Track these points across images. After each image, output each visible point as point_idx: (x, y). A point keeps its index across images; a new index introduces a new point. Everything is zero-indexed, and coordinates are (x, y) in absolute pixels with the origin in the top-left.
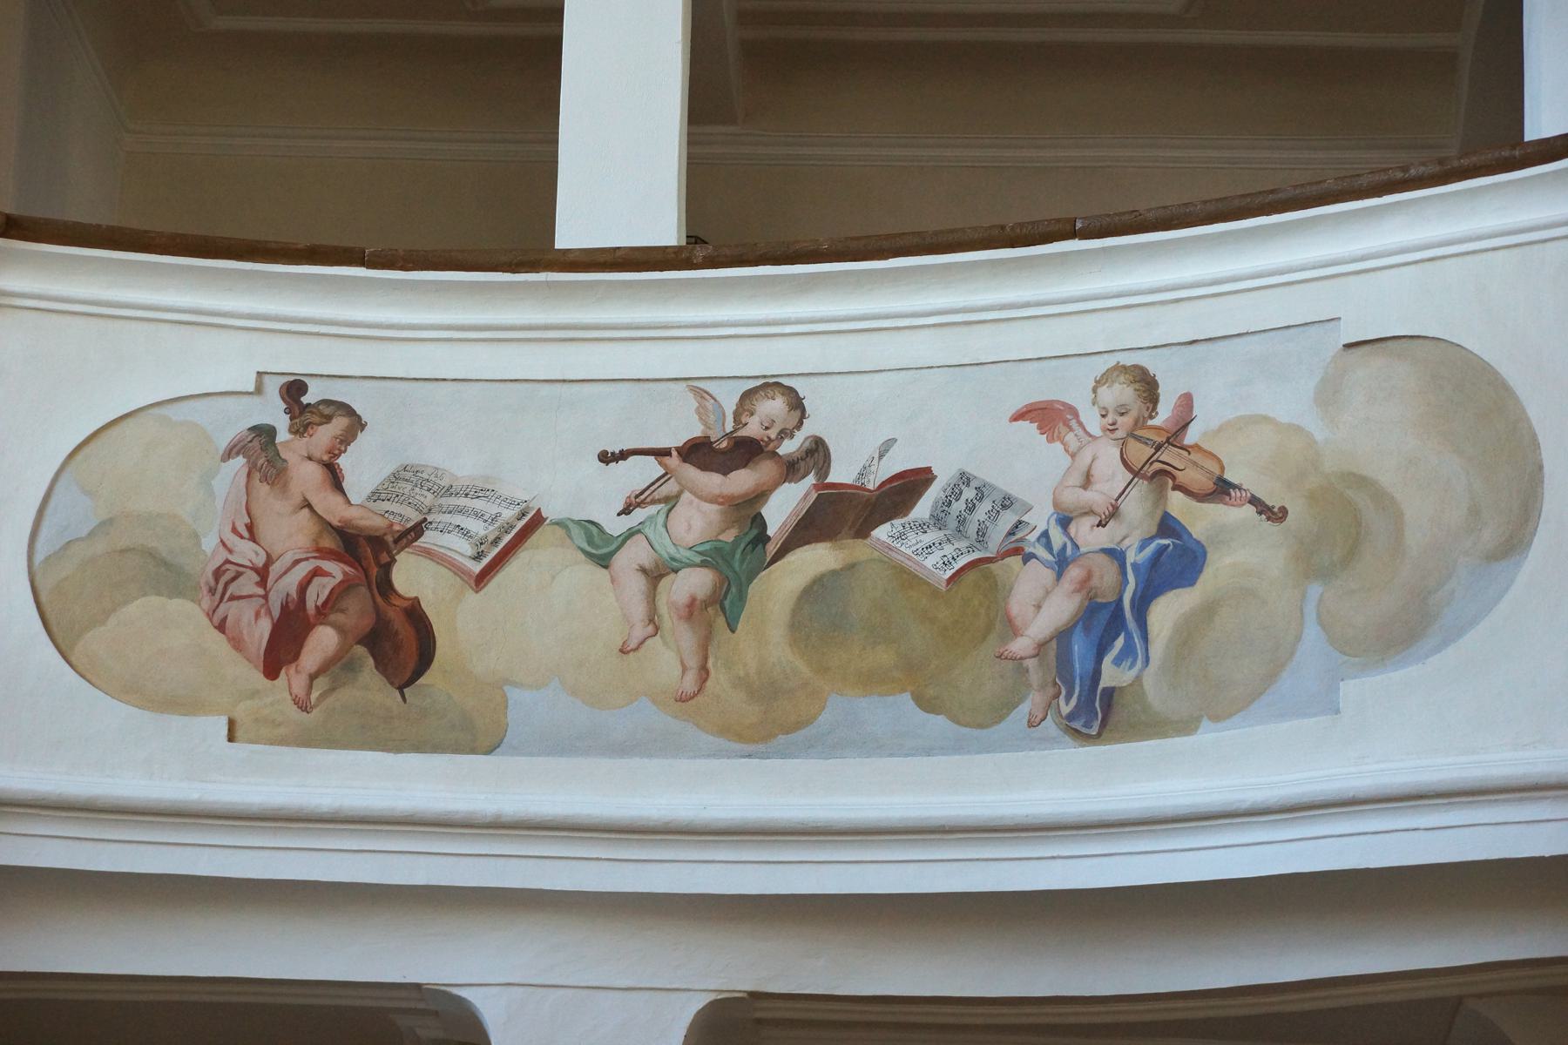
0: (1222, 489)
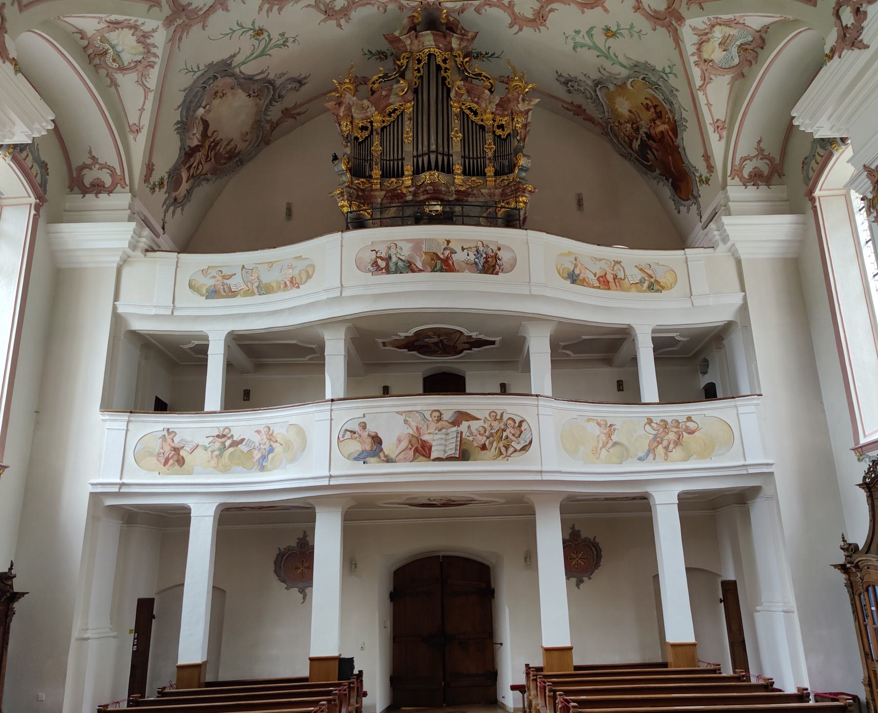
0: (276, 441)
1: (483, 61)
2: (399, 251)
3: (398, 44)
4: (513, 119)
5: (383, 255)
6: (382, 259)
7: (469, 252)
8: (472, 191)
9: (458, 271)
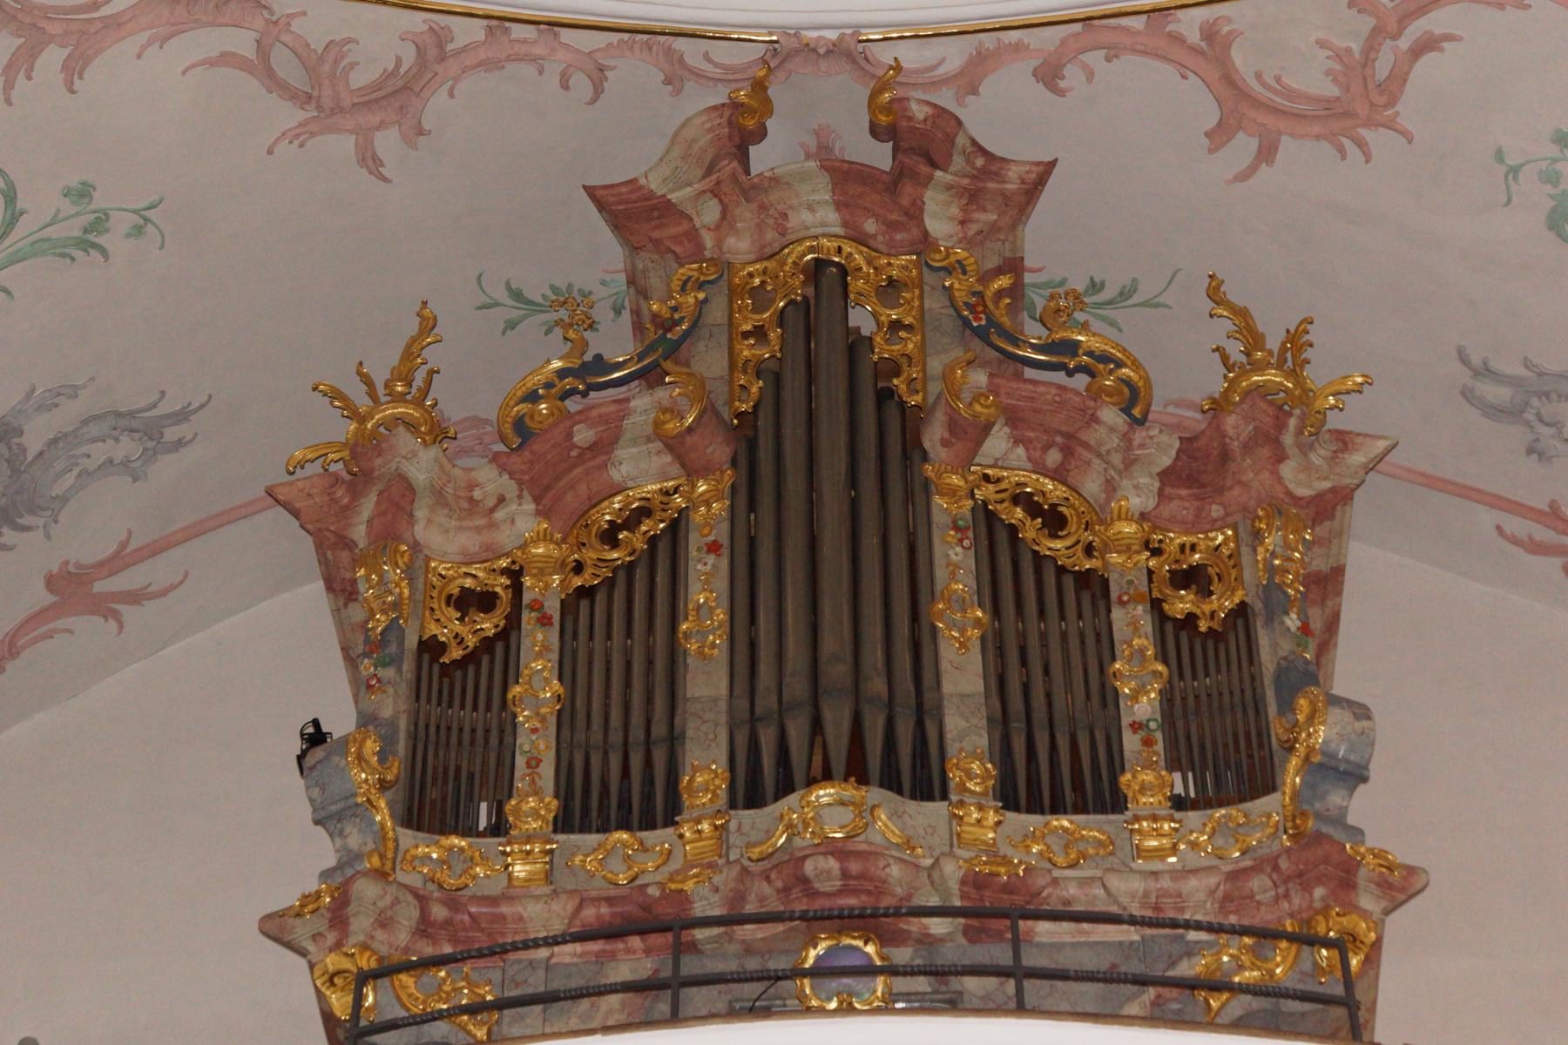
3: (659, 227)
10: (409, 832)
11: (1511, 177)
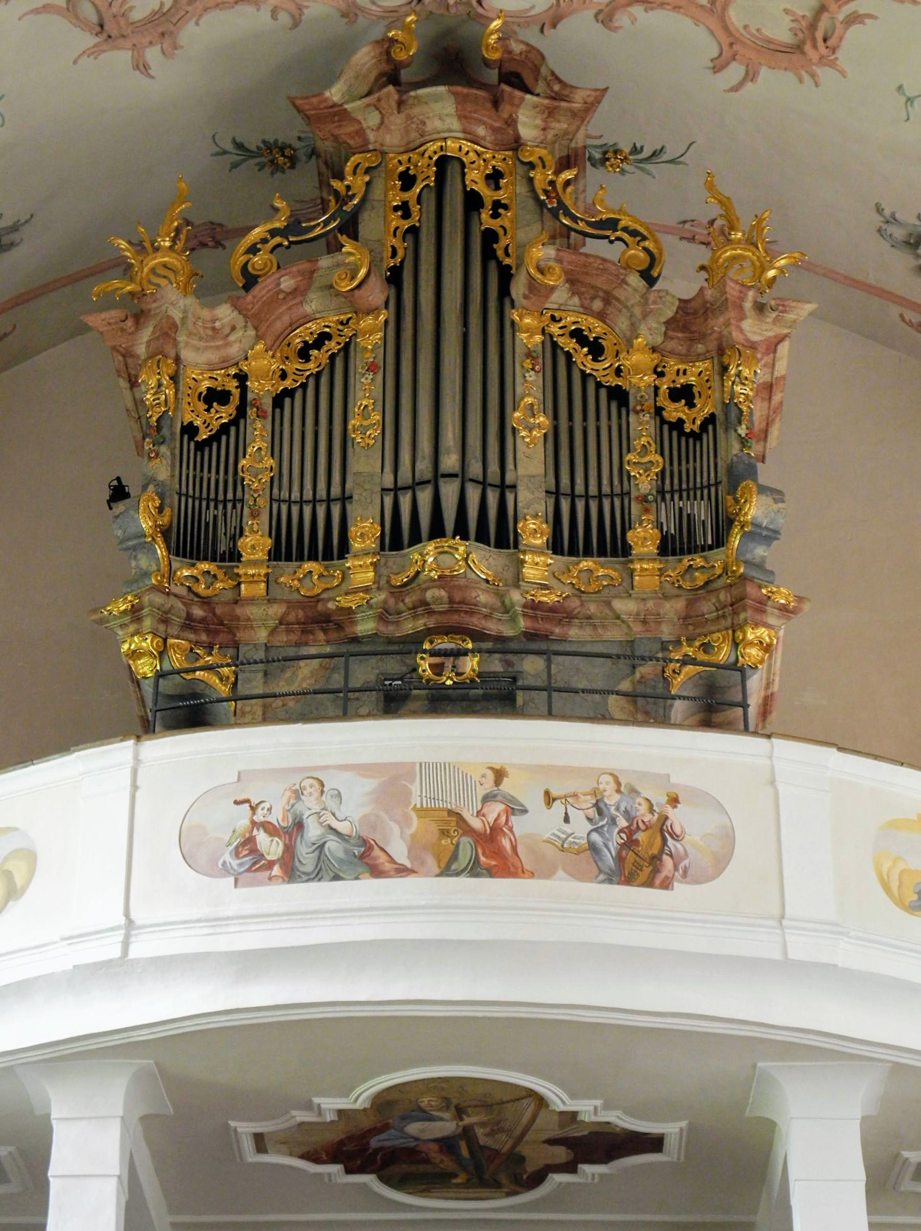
1: (623, 172)
2: (331, 804)
4: (725, 369)
5: (277, 817)
6: (271, 829)
7: (571, 811)
8: (582, 605)
9: (532, 875)
10: (178, 558)
11: (909, 104)
